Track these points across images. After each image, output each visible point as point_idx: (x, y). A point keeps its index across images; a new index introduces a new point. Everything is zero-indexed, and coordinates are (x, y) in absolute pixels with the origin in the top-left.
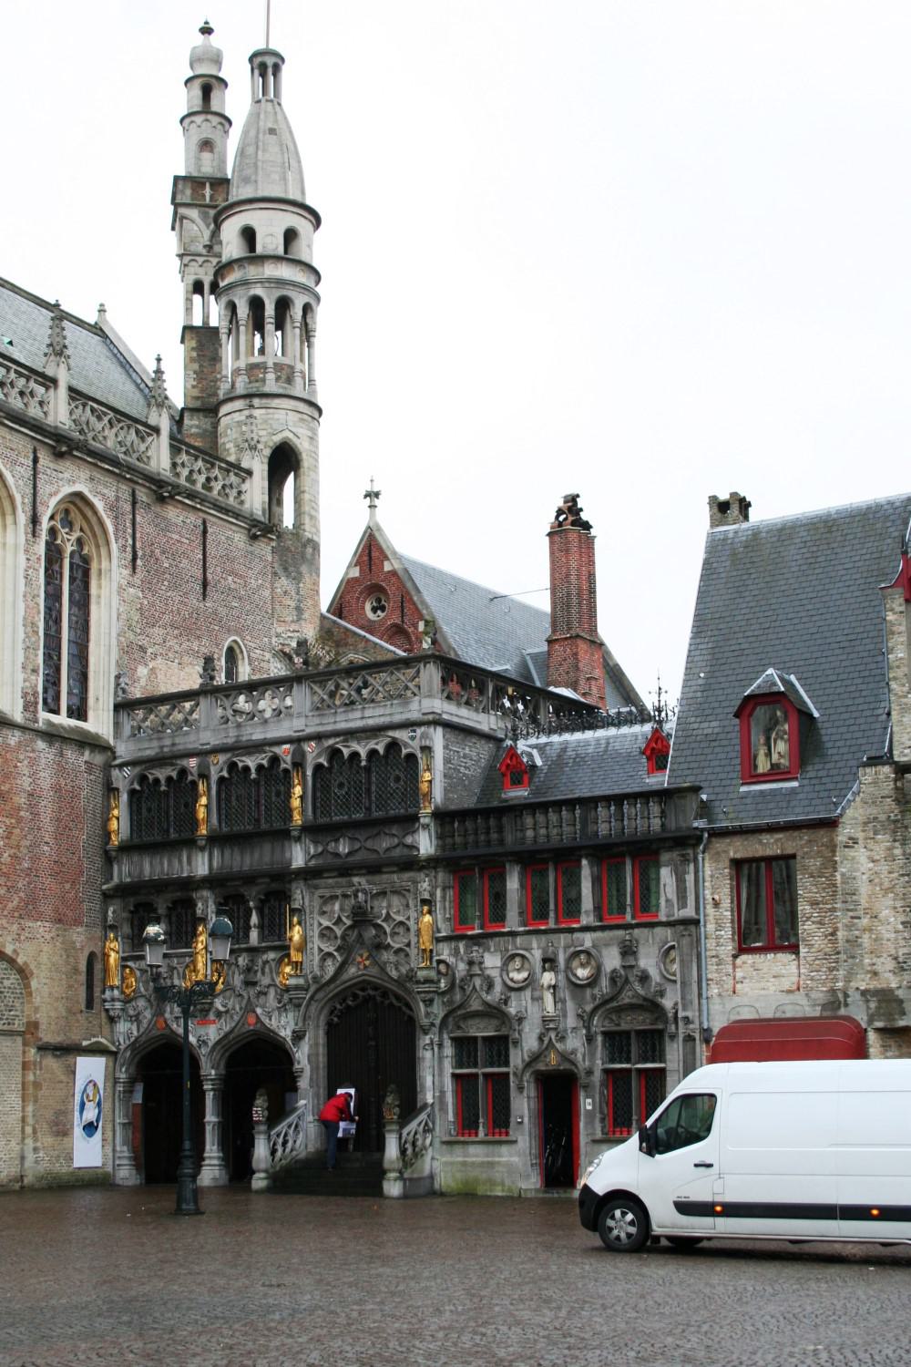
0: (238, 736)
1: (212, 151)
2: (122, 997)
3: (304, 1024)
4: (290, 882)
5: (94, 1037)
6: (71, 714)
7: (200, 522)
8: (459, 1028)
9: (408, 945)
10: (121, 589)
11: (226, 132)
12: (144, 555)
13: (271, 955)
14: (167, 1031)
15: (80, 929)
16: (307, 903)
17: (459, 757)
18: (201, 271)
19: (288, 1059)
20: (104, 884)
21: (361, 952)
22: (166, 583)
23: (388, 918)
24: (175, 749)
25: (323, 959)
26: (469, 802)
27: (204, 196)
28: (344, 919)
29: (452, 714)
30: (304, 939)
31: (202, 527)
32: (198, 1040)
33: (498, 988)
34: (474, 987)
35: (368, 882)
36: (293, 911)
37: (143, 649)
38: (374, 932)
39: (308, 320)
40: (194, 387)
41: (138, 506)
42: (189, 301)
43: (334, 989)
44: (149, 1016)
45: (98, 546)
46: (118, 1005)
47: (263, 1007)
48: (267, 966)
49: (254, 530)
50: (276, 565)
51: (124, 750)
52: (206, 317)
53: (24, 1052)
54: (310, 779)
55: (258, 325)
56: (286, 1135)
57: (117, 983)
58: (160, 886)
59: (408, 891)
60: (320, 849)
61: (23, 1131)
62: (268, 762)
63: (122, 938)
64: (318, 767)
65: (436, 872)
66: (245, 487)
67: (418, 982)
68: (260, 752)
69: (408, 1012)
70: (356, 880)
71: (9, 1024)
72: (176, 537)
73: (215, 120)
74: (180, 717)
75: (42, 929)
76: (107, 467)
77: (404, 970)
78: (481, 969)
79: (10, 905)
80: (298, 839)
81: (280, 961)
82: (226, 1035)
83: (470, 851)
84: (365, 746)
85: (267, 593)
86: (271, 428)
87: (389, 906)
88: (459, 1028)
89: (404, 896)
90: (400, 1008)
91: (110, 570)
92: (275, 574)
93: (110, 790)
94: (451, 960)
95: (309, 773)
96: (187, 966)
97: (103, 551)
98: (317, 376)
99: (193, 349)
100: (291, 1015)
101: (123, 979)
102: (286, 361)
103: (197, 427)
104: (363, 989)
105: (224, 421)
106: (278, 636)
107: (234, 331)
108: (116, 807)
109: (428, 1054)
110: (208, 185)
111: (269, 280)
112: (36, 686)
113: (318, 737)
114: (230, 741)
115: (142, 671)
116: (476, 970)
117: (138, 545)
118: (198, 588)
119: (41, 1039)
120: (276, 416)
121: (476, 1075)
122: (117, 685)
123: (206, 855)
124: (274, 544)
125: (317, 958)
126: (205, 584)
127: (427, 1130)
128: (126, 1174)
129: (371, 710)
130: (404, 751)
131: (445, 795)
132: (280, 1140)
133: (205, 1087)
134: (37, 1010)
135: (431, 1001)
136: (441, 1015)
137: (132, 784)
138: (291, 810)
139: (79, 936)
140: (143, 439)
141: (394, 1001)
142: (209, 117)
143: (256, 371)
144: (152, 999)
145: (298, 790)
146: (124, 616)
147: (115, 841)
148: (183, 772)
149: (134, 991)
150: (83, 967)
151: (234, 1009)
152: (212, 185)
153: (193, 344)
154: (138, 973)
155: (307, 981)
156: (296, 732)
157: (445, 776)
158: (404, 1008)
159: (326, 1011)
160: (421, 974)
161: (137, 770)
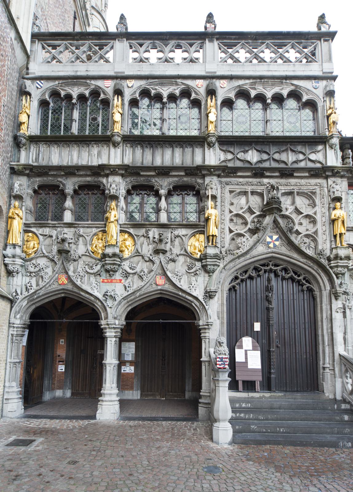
2: (23, 255)
4: (203, 177)
9: (316, 232)
13: (182, 232)
14: (70, 287)
21: (270, 234)
43: (242, 262)
57: (19, 242)
90: (299, 281)
133: (108, 334)
141: (294, 275)
159: (230, 279)
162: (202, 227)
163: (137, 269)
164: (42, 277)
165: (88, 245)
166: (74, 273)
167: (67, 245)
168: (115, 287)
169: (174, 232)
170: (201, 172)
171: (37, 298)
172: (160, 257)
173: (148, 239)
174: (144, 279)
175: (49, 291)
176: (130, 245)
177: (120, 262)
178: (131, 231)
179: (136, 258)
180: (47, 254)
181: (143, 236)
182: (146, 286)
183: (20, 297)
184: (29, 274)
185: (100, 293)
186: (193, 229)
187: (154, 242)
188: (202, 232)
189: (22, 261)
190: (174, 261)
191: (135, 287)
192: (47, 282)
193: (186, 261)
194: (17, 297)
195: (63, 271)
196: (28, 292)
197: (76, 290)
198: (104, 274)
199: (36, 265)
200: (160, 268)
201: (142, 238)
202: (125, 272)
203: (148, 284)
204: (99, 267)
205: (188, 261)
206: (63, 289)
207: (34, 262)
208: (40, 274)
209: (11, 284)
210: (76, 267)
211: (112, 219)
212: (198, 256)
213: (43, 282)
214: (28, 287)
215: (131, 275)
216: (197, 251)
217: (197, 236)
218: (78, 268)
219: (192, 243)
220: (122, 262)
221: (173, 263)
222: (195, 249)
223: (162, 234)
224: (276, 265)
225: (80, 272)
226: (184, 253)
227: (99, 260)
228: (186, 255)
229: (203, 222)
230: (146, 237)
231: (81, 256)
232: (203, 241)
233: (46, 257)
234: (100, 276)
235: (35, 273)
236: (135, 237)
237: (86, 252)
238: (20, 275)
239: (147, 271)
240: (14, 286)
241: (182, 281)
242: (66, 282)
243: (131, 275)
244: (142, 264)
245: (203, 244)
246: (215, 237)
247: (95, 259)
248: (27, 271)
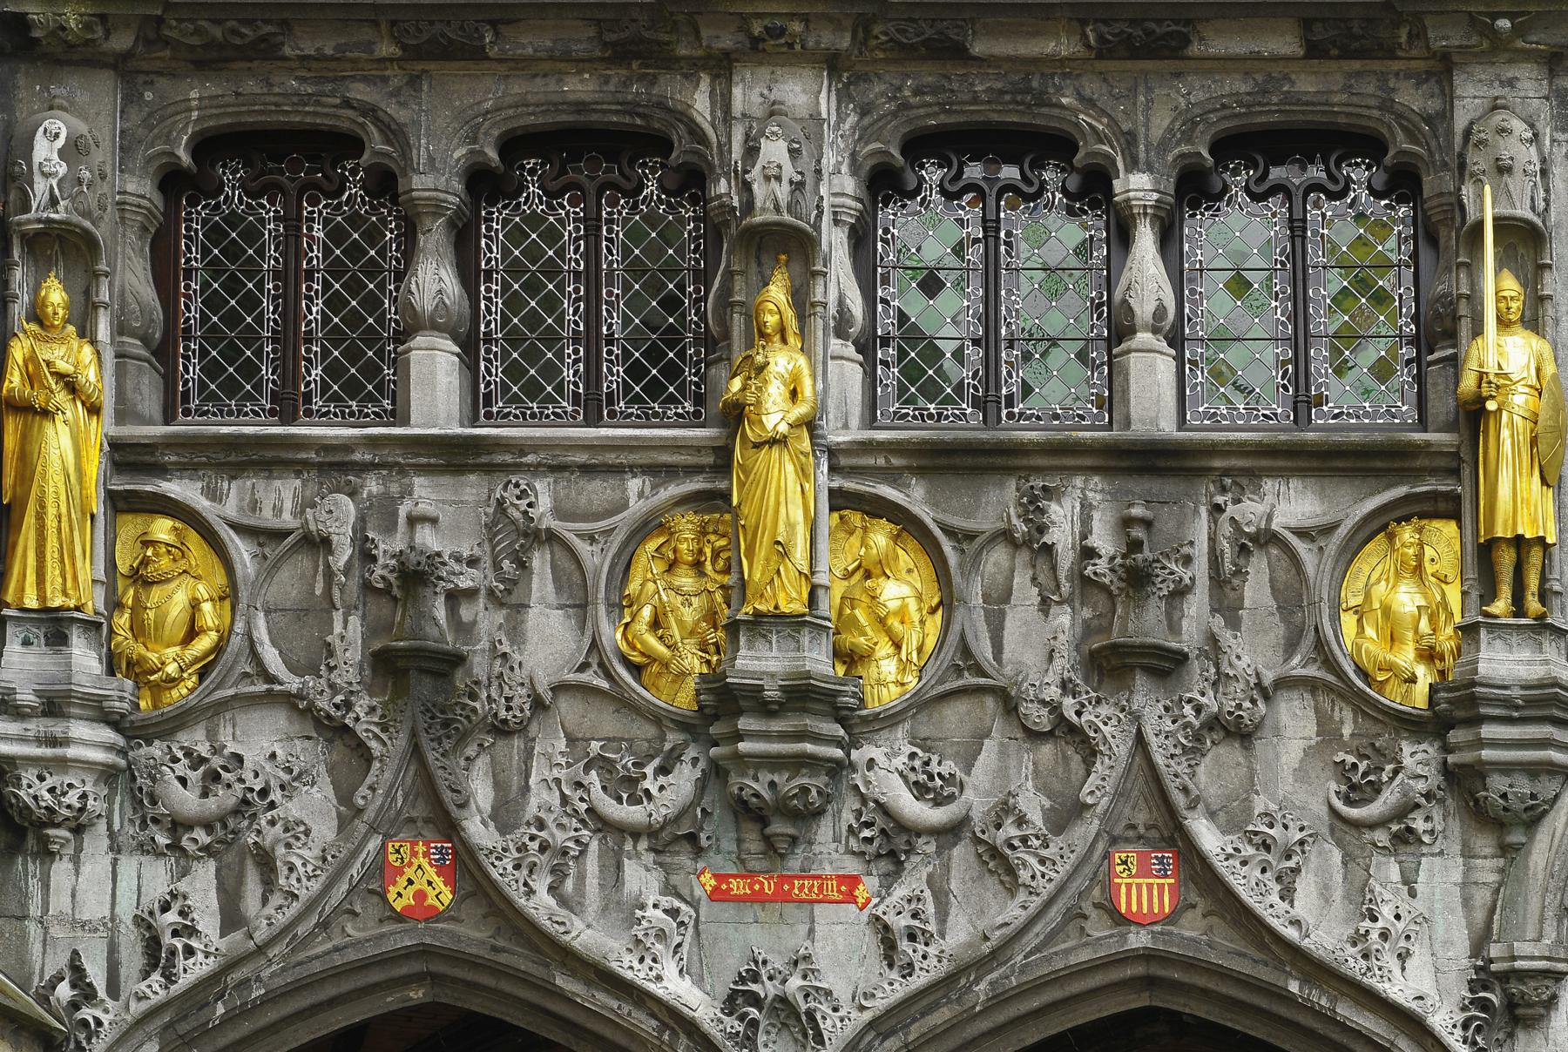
14: (473, 934)
32: (732, 1003)
44: (324, 831)
47: (1233, 820)
63: (120, 329)
144: (363, 716)
151: (1005, 810)
154: (242, 551)
162: (1442, 463)
163: (969, 795)
164: (265, 862)
165: (602, 609)
166: (503, 829)
167: (441, 613)
168: (811, 931)
169: (1231, 509)
170: (1418, 35)
171: (227, 1020)
172: (1138, 701)
173: (1043, 565)
174: (1024, 875)
175: (317, 967)
176: (913, 605)
177: (838, 743)
178: (914, 497)
180: (293, 683)
181: (1006, 535)
183: (106, 1015)
184: (162, 840)
185: (699, 982)
186: (1373, 482)
187: (1086, 583)
188: (1447, 507)
190: (1239, 732)
191: (959, 935)
192: (303, 894)
193: (1328, 732)
194: (87, 1013)
195: (419, 811)
196: (170, 978)
197: (521, 961)
198: (719, 832)
199: (216, 762)
200: (1139, 784)
201: (998, 557)
202: (880, 821)
203: (1055, 914)
204: (684, 780)
205: (1347, 731)
206: (423, 952)
207: (196, 739)
208: (251, 838)
209: (34, 910)
210: (516, 781)
211: (776, 414)
212: (1419, 696)
213: (276, 899)
214: (167, 939)
215: (928, 846)
216: (1405, 656)
217: (1407, 534)
218: (526, 789)
219: (1368, 596)
220: (855, 744)
221: (1230, 753)
222: (1393, 639)
223: (1147, 524)
225: (549, 819)
226: (1312, 671)
227: (683, 725)
228: (1329, 688)
229: (1450, 427)
230: (1027, 543)
231: (547, 697)
232: (1452, 573)
233: (290, 701)
234: (699, 852)
235: (208, 827)
236: (947, 546)
237: (583, 667)
238: (96, 843)
239: (1048, 814)
240: (56, 931)
242: (447, 896)
243: (928, 846)
244: (1003, 752)
245: (1454, 595)
246: (1535, 557)
247: (657, 718)
248: (151, 812)
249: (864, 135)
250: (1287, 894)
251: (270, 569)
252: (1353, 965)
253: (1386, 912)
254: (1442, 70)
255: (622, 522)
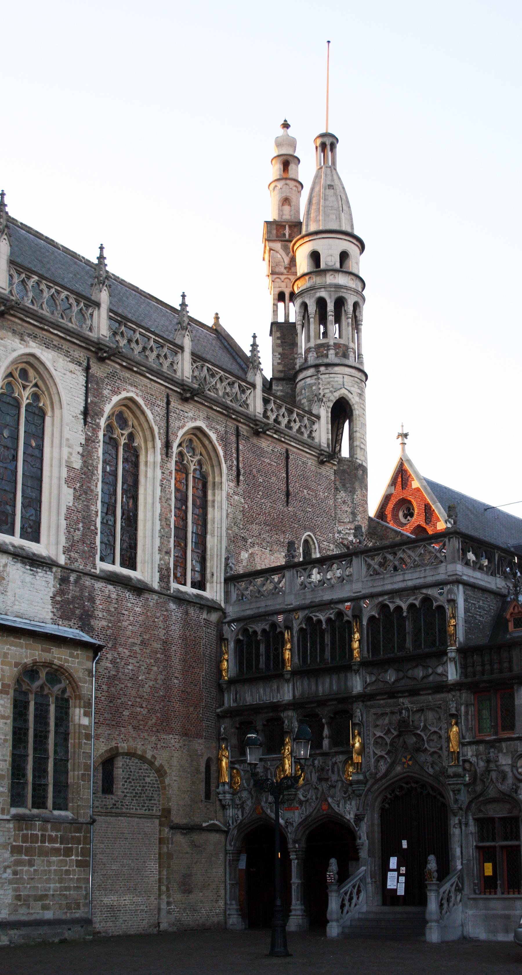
0: (312, 598)
1: (290, 205)
2: (231, 791)
3: (364, 809)
5: (211, 820)
6: (193, 585)
7: (284, 451)
8: (480, 811)
9: (441, 749)
10: (229, 497)
11: (299, 192)
12: (245, 473)
15: (200, 741)
16: (364, 719)
17: (476, 608)
18: (284, 285)
19: (352, 835)
20: (218, 708)
21: (405, 754)
22: (260, 493)
23: (425, 728)
24: (268, 609)
25: (377, 761)
26: (484, 641)
27: (284, 235)
28: (392, 730)
29: (469, 576)
30: (363, 745)
31: (285, 455)
32: (286, 822)
33: (510, 780)
34: (492, 779)
35: (409, 702)
36: (354, 725)
37: (244, 539)
38: (415, 739)
39: (357, 314)
40: (279, 364)
41: (240, 438)
42: (275, 305)
45: (212, 466)
46: (228, 796)
48: (336, 766)
49: (321, 457)
50: (337, 483)
51: (232, 611)
52: (287, 316)
53: (160, 831)
54: (365, 627)
55: (323, 319)
56: (351, 893)
58: (256, 709)
59: (440, 708)
60: (374, 679)
61: (160, 889)
62: (335, 615)
64: (372, 619)
65: (461, 694)
66: (315, 427)
67: (449, 777)
68: (329, 609)
69: (441, 799)
70: (401, 700)
71: (149, 810)
72: (268, 461)
73: (292, 184)
74: (270, 586)
75: (174, 740)
76: (218, 409)
77: (438, 769)
78: (497, 766)
79: (150, 723)
80: (357, 672)
81: (345, 763)
82: (306, 818)
83: (485, 677)
84: (406, 601)
85: (331, 502)
86: (333, 387)
87: (425, 720)
88: (480, 811)
89: (437, 712)
91: (221, 483)
92: (336, 489)
93: (221, 639)
94: (473, 760)
95: (365, 622)
96: (278, 767)
97: (216, 470)
98: (364, 352)
99: (278, 338)
100: (353, 803)
101: (231, 777)
102: (342, 342)
103: (282, 391)
104: (407, 783)
105: (300, 385)
106: (339, 532)
107: (306, 325)
108: (227, 653)
109: (457, 831)
110: (287, 227)
111: (331, 285)
112: (169, 563)
113: (371, 596)
114: (308, 602)
115: (244, 555)
116: (492, 766)
117: (241, 465)
118: (283, 497)
119: (172, 821)
120: (336, 379)
121: (494, 847)
122: (227, 565)
123: (291, 685)
124: (335, 468)
125: (373, 760)
126: (288, 494)
127: (459, 890)
128: (234, 920)
129: (410, 575)
130: (435, 604)
131: (466, 635)
132: (347, 897)
134: (169, 800)
135: (459, 790)
136: (467, 801)
137: (237, 635)
138: (351, 650)
139: (199, 745)
140: (243, 392)
141: (431, 792)
142: (288, 182)
143: (322, 349)
145: (357, 636)
146: (231, 516)
147: (226, 676)
148: (274, 625)
149: (239, 786)
150: (203, 769)
151: (312, 799)
152: (290, 227)
153: (278, 335)
154: (242, 773)
155: (365, 777)
156: (354, 593)
157: (466, 622)
158: (438, 797)
159: (379, 800)
160: (451, 771)
161: (241, 625)
179: (307, 786)
181: (311, 765)
182: (315, 812)
189: (230, 795)
203: (316, 810)
207: (239, 794)
215: (304, 803)
224: (417, 782)
238: (231, 807)
241: (341, 805)
249: (298, 717)
250: (339, 807)
251: (245, 774)
252: (343, 815)
253: (347, 808)
254: (352, 703)
255: (276, 766)
